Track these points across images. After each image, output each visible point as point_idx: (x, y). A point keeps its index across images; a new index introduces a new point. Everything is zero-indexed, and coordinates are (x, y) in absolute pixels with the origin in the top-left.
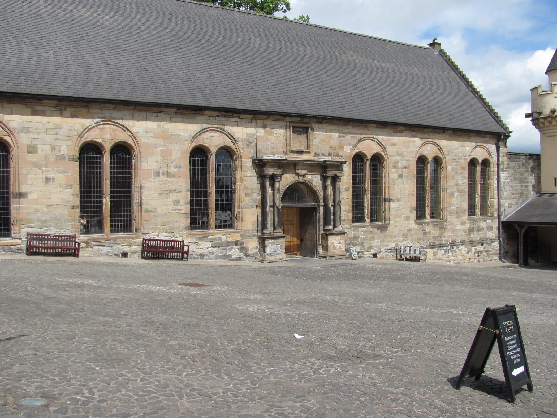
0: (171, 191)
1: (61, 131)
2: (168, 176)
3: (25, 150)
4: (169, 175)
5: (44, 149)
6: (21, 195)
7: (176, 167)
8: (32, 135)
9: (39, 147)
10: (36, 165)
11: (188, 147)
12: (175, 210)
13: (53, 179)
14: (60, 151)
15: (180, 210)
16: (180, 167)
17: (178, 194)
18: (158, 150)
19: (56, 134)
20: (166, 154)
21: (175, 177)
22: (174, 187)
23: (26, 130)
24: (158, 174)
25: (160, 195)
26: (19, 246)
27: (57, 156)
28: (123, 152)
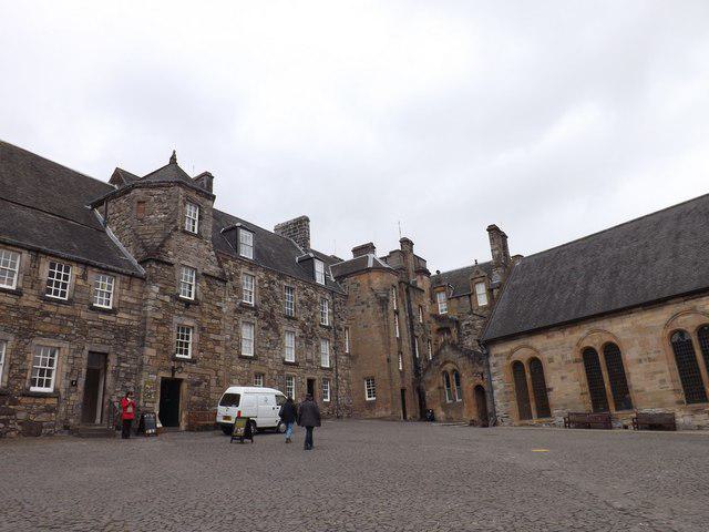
0: (655, 373)
4: (650, 360)
5: (557, 358)
6: (550, 390)
7: (655, 352)
10: (554, 369)
11: (663, 333)
18: (636, 342)
23: (545, 349)
25: (646, 377)
28: (612, 351)
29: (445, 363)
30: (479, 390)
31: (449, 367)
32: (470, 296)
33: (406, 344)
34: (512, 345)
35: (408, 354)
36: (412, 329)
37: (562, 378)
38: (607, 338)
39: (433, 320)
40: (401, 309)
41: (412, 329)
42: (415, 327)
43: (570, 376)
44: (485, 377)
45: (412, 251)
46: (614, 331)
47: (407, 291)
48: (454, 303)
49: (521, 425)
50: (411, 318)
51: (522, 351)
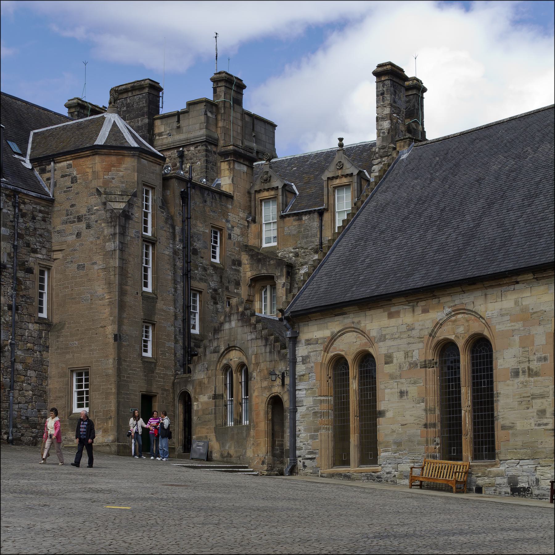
0: (534, 397)
1: (415, 333)
2: (530, 375)
3: (383, 361)
4: (531, 373)
5: (398, 357)
7: (539, 360)
8: (389, 343)
9: (395, 355)
10: (392, 377)
12: (539, 425)
13: (407, 392)
14: (412, 357)
15: (546, 424)
16: (545, 359)
17: (543, 400)
18: (517, 338)
19: (409, 337)
20: (526, 342)
21: (539, 376)
22: (537, 391)
23: (383, 338)
24: (516, 373)
26: (379, 474)
27: (410, 364)
28: (481, 346)
29: (229, 349)
30: (276, 402)
31: (235, 357)
32: (321, 213)
33: (167, 308)
34: (333, 326)
35: (169, 326)
36: (187, 275)
37: (402, 394)
38: (476, 327)
39: (245, 259)
40: (164, 236)
41: (187, 275)
42: (198, 273)
43: (413, 391)
44: (287, 381)
45: (238, 102)
46: (487, 314)
47: (184, 197)
48: (291, 224)
49: (332, 476)
50: (188, 252)
51: (345, 336)
